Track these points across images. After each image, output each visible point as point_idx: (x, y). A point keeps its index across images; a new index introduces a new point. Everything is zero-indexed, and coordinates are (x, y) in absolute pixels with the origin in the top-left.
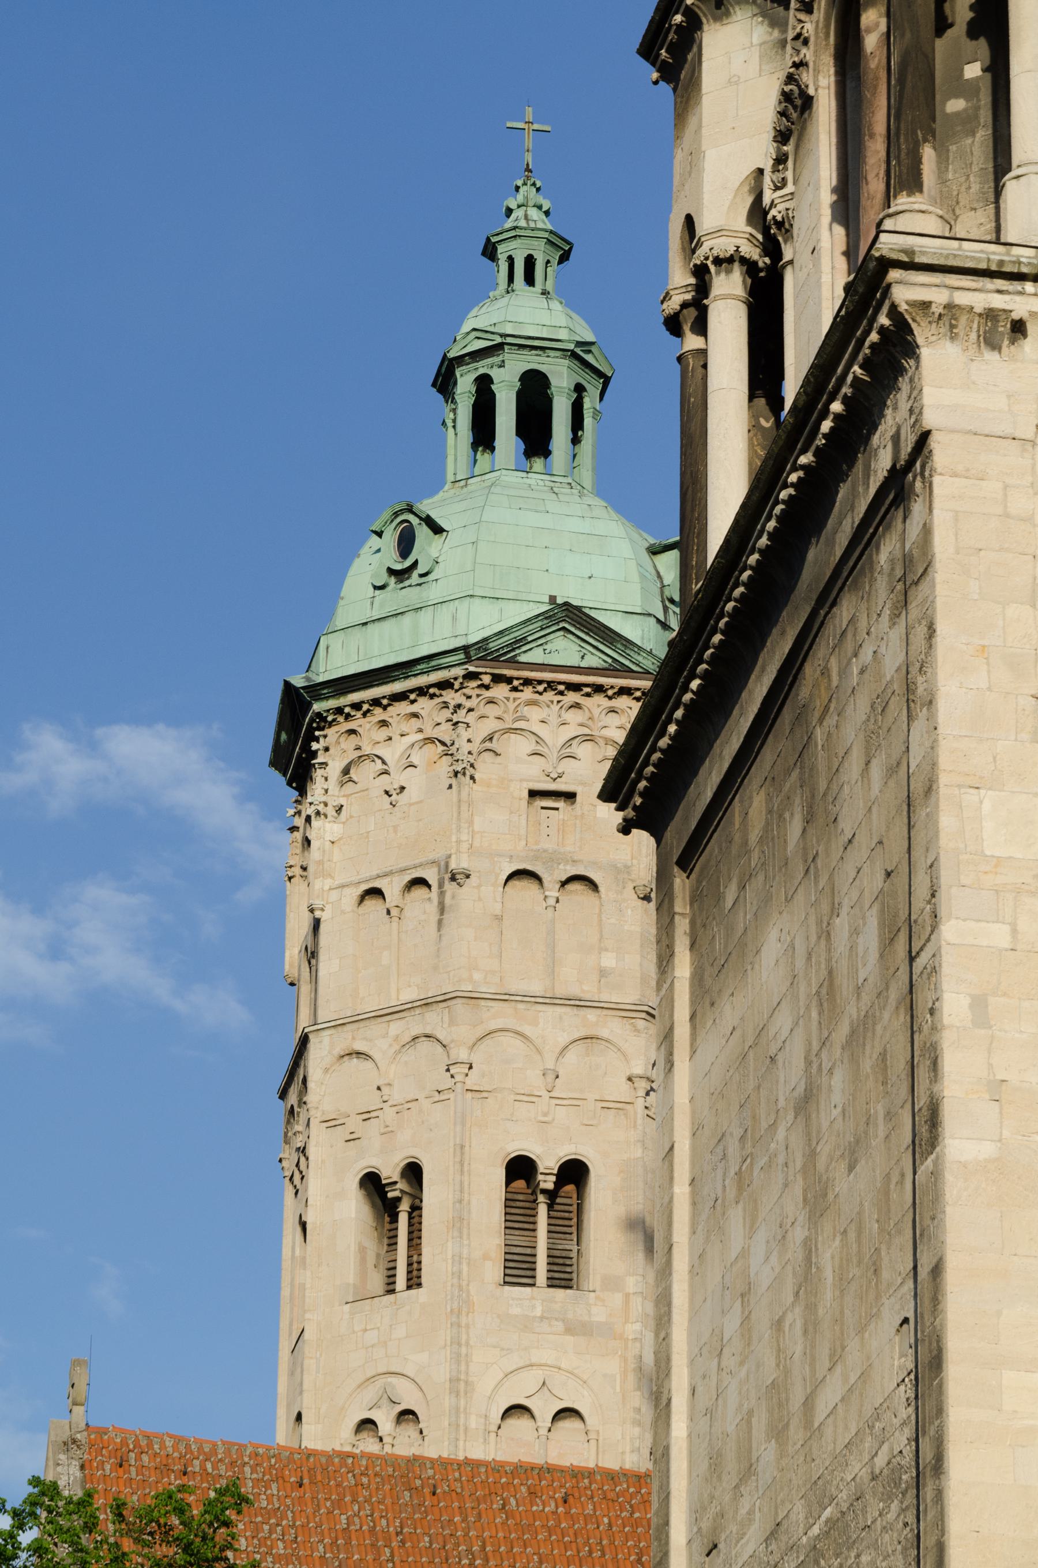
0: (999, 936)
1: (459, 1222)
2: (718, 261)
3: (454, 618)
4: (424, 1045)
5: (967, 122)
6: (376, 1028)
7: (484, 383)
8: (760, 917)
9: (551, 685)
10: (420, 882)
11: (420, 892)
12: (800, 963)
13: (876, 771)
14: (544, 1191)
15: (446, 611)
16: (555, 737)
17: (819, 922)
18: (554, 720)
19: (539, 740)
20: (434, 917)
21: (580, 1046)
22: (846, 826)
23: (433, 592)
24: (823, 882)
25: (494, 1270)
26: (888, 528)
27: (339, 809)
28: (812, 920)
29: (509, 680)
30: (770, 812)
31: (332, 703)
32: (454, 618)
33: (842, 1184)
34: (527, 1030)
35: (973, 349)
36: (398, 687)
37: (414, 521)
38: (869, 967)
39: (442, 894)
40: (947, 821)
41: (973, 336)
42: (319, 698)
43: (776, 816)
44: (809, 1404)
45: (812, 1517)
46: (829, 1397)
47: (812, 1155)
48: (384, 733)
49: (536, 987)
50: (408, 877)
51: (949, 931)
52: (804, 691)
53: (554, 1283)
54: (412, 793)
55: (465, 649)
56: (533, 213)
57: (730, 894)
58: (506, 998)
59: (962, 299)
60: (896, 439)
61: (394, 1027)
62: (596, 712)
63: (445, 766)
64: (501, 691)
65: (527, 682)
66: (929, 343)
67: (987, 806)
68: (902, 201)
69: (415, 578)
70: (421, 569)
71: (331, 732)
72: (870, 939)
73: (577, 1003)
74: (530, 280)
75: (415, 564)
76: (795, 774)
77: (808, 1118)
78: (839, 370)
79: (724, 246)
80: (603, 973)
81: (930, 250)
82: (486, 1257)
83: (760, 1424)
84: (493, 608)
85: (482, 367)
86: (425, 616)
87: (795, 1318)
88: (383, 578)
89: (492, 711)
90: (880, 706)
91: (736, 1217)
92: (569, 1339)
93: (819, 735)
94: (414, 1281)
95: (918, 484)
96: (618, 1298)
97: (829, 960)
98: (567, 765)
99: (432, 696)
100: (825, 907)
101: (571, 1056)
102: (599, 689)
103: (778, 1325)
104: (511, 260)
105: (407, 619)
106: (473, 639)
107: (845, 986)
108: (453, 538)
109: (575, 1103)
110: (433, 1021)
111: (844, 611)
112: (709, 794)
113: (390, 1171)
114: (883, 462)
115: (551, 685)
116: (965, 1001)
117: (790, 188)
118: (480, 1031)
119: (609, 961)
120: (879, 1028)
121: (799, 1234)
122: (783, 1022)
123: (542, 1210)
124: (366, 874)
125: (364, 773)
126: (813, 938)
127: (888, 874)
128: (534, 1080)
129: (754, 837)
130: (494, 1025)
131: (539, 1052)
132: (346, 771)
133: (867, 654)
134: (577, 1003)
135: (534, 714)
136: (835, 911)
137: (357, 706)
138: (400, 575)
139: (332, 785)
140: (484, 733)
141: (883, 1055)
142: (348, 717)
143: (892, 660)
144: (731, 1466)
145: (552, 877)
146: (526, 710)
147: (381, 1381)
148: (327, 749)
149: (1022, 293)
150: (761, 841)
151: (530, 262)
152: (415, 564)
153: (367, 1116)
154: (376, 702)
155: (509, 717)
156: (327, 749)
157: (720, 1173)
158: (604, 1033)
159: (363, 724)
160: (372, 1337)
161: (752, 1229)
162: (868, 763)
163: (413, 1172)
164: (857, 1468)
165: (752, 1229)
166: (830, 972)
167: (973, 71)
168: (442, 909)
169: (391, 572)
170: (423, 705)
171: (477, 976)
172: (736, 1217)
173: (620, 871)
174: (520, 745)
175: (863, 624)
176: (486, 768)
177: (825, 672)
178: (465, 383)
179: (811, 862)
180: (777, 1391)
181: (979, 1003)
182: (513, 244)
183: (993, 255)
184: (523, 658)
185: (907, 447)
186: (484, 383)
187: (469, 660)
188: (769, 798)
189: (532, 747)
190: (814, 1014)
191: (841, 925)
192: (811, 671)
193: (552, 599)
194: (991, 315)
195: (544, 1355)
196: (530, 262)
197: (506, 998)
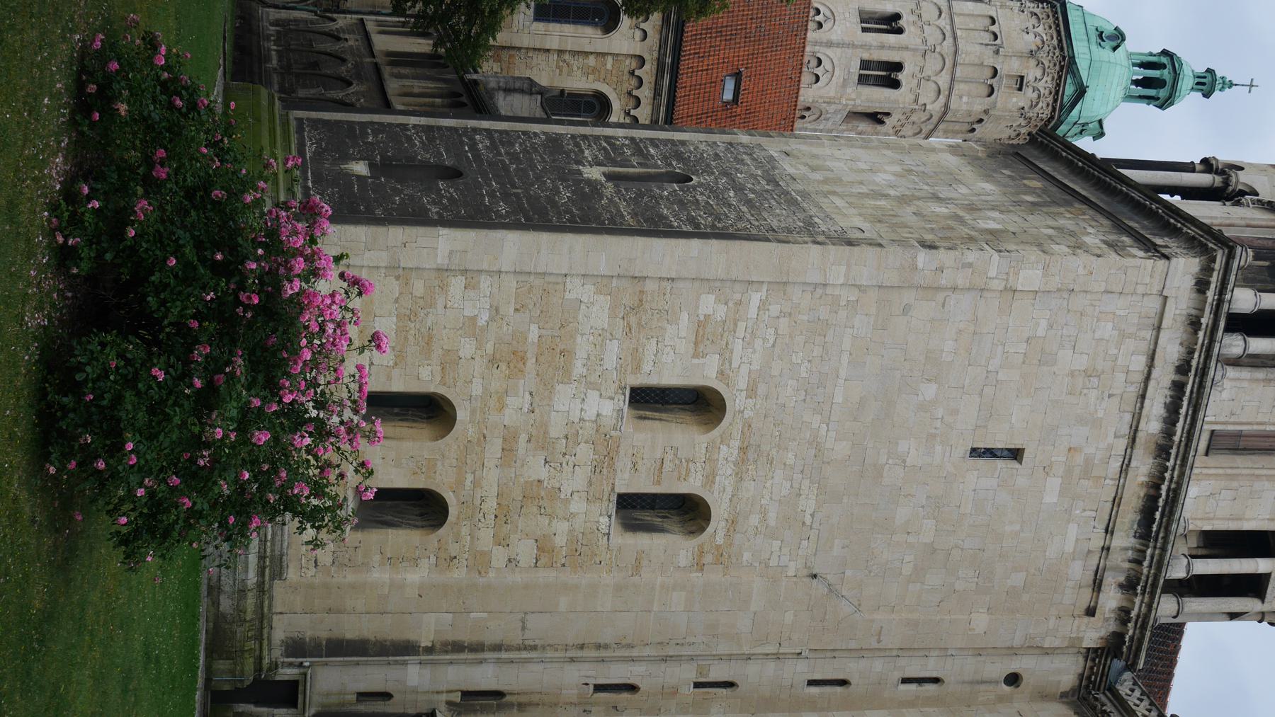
1: (882, 47)
2: (1227, 179)
3: (1084, 54)
4: (941, 37)
6: (948, 21)
7: (1162, 66)
8: (998, 183)
9: (1058, 85)
10: (996, 37)
11: (992, 37)
12: (983, 198)
13: (1050, 231)
14: (890, 75)
15: (1087, 51)
16: (1041, 85)
17: (997, 206)
18: (1047, 85)
19: (1040, 80)
20: (984, 42)
21: (936, 89)
22: (1030, 218)
23: (1094, 47)
24: (1011, 208)
25: (866, 56)
26: (1135, 241)
27: (1023, 11)
28: (998, 203)
29: (1062, 71)
30: (1035, 188)
31: (1059, 10)
32: (1084, 54)
33: (909, 210)
34: (944, 71)
35: (1197, 276)
36: (1063, 33)
37: (1119, 41)
38: (982, 224)
39: (992, 45)
41: (1201, 277)
42: (1061, 6)
43: (1032, 191)
44: (834, 193)
45: (798, 192)
46: (839, 202)
47: (919, 199)
48: (1047, 27)
49: (958, 74)
50: (998, 34)
52: (1077, 205)
53: (860, 76)
54: (1026, 36)
55: (1074, 57)
56: (1221, 86)
57: (1007, 172)
58: (954, 65)
59: (1215, 274)
60: (1166, 247)
61: (948, 27)
62: (1048, 99)
63: (1034, 48)
64: (1057, 68)
65: (1060, 77)
66: (1200, 261)
67: (1038, 272)
68: (1250, 252)
69: (1099, 41)
70: (1102, 43)
71: (1049, 10)
72: (992, 225)
73: (951, 88)
74: (1198, 84)
75: (1103, 41)
76: (1048, 199)
77: (931, 198)
78: (1192, 228)
80: (961, 97)
82: (871, 54)
83: (828, 174)
84: (1087, 67)
85: (1169, 66)
86: (1086, 44)
87: (864, 189)
88: (1099, 30)
89: (1051, 65)
90: (1072, 234)
91: (898, 169)
92: (842, 80)
93: (1062, 210)
94: (864, 30)
95: (1150, 254)
96: (853, 96)
97: (985, 209)
98: (1031, 90)
99: (1058, 45)
100: (1003, 208)
101: (934, 86)
102: (1055, 101)
103: (861, 183)
104: (1205, 77)
105: (1085, 37)
106: (1077, 60)
107: (976, 214)
108: (1111, 53)
109: (919, 86)
110: (949, 40)
111: (1105, 222)
112: (1041, 166)
113: (902, 23)
114: (1159, 241)
115: (1058, 85)
116: (971, 261)
117: (1251, 205)
118: (945, 56)
119: (965, 99)
120: (962, 227)
121: (892, 192)
123: (883, 73)
124: (1001, 19)
125: (1034, 21)
126: (993, 204)
127: (1014, 233)
128: (928, 72)
129: (1026, 182)
130: (947, 60)
131: (937, 75)
132: (1036, 14)
133: (1090, 230)
134: (951, 88)
135: (1049, 79)
136: (1002, 212)
137: (1057, 19)
138: (1101, 35)
139: (1031, 10)
140: (1044, 62)
141: (952, 228)
142: (1054, 16)
143: (1088, 240)
144: (815, 162)
145: (994, 82)
146: (1051, 75)
147: (831, 17)
148: (1043, 8)
149: (1215, 295)
150: (1025, 185)
151: (1203, 84)
152: (1103, 41)
153: (920, 16)
154: (1058, 25)
155: (1050, 71)
156: (1043, 8)
157: (913, 163)
158: (941, 97)
159: (1051, 20)
160: (847, 15)
161: (895, 175)
162: (1053, 228)
163: (900, 31)
164: (813, 211)
165: (895, 175)
166: (981, 209)
168: (987, 45)
169: (1102, 32)
170: (1055, 42)
171: (964, 56)
172: (898, 169)
173: (994, 105)
174: (1038, 73)
175: (1101, 229)
176: (1033, 62)
177: (1084, 214)
178: (1164, 60)
179: (1019, 203)
180: (838, 181)
181: (970, 265)
182: (1210, 79)
184: (1069, 76)
185: (1163, 250)
186: (1162, 66)
187: (1069, 58)
188: (1040, 188)
189: (1038, 78)
190: (966, 202)
191: (996, 214)
193: (1088, 87)
194: (1209, 283)
195: (837, 73)
196: (1203, 84)
197: (954, 65)
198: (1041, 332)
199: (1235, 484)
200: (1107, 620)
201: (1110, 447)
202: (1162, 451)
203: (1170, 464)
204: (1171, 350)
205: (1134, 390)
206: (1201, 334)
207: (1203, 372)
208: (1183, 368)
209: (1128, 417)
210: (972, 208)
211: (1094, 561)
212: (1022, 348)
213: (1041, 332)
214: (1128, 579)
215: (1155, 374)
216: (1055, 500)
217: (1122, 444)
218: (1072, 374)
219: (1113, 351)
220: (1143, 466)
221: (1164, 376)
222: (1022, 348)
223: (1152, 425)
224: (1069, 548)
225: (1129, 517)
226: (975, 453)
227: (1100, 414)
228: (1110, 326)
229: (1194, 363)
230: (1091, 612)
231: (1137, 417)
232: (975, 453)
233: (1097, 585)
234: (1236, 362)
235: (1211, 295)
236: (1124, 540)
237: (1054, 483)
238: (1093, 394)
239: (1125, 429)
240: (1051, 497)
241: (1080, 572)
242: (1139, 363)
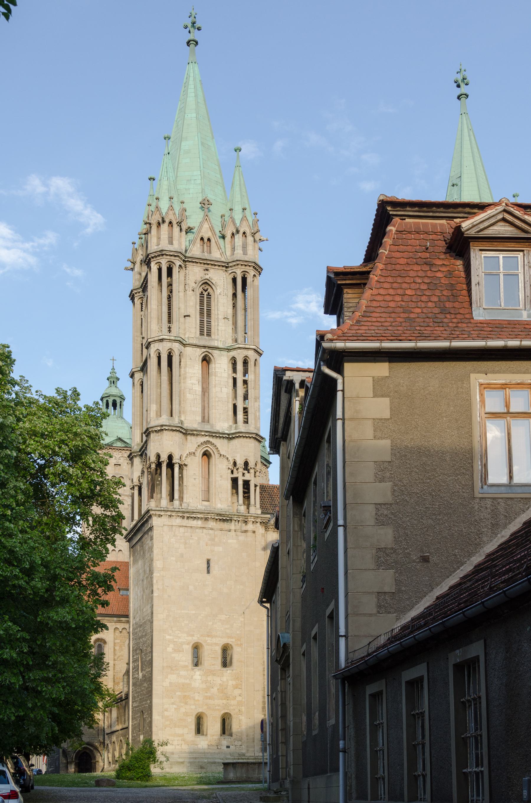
0: (159, 575)
5: (159, 485)
38: (148, 572)
40: (154, 564)
51: (154, 574)
68: (152, 500)
79: (136, 484)
81: (154, 509)
90: (149, 548)
111: (146, 536)
122: (141, 571)
133: (148, 542)
167: (159, 479)
181: (157, 581)
183: (159, 509)
192: (144, 538)
198: (174, 559)
199: (217, 493)
200: (256, 527)
201: (206, 534)
202: (206, 519)
203: (210, 517)
204: (178, 521)
205: (189, 530)
206: (173, 514)
207: (183, 512)
208: (183, 517)
209: (197, 530)
210: (145, 571)
211: (239, 533)
212: (179, 563)
213: (174, 559)
214: (244, 523)
215: (184, 525)
216: (221, 548)
217: (204, 530)
218: (185, 548)
219: (179, 537)
220: (211, 524)
221: (185, 522)
222: (179, 563)
223: (199, 523)
224: (235, 541)
225: (225, 526)
226: (208, 572)
227: (197, 538)
228: (172, 540)
229: (181, 515)
230: (254, 532)
231: (197, 528)
232: (208, 572)
233: (246, 531)
234: (181, 498)
235: (162, 513)
236: (232, 526)
237: (217, 549)
238: (191, 541)
239: (201, 530)
240: (221, 549)
241: (242, 537)
242: (182, 530)
